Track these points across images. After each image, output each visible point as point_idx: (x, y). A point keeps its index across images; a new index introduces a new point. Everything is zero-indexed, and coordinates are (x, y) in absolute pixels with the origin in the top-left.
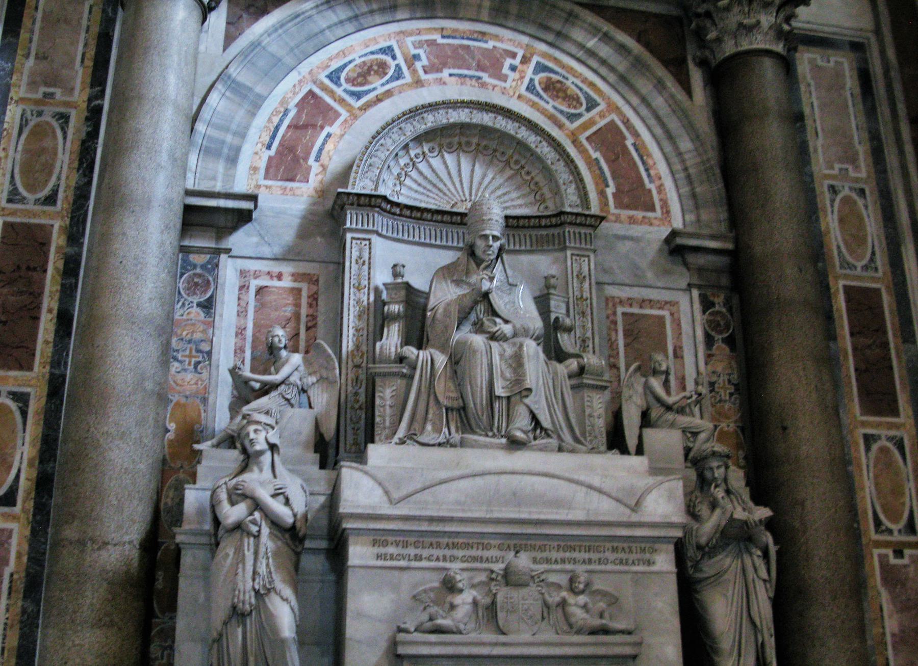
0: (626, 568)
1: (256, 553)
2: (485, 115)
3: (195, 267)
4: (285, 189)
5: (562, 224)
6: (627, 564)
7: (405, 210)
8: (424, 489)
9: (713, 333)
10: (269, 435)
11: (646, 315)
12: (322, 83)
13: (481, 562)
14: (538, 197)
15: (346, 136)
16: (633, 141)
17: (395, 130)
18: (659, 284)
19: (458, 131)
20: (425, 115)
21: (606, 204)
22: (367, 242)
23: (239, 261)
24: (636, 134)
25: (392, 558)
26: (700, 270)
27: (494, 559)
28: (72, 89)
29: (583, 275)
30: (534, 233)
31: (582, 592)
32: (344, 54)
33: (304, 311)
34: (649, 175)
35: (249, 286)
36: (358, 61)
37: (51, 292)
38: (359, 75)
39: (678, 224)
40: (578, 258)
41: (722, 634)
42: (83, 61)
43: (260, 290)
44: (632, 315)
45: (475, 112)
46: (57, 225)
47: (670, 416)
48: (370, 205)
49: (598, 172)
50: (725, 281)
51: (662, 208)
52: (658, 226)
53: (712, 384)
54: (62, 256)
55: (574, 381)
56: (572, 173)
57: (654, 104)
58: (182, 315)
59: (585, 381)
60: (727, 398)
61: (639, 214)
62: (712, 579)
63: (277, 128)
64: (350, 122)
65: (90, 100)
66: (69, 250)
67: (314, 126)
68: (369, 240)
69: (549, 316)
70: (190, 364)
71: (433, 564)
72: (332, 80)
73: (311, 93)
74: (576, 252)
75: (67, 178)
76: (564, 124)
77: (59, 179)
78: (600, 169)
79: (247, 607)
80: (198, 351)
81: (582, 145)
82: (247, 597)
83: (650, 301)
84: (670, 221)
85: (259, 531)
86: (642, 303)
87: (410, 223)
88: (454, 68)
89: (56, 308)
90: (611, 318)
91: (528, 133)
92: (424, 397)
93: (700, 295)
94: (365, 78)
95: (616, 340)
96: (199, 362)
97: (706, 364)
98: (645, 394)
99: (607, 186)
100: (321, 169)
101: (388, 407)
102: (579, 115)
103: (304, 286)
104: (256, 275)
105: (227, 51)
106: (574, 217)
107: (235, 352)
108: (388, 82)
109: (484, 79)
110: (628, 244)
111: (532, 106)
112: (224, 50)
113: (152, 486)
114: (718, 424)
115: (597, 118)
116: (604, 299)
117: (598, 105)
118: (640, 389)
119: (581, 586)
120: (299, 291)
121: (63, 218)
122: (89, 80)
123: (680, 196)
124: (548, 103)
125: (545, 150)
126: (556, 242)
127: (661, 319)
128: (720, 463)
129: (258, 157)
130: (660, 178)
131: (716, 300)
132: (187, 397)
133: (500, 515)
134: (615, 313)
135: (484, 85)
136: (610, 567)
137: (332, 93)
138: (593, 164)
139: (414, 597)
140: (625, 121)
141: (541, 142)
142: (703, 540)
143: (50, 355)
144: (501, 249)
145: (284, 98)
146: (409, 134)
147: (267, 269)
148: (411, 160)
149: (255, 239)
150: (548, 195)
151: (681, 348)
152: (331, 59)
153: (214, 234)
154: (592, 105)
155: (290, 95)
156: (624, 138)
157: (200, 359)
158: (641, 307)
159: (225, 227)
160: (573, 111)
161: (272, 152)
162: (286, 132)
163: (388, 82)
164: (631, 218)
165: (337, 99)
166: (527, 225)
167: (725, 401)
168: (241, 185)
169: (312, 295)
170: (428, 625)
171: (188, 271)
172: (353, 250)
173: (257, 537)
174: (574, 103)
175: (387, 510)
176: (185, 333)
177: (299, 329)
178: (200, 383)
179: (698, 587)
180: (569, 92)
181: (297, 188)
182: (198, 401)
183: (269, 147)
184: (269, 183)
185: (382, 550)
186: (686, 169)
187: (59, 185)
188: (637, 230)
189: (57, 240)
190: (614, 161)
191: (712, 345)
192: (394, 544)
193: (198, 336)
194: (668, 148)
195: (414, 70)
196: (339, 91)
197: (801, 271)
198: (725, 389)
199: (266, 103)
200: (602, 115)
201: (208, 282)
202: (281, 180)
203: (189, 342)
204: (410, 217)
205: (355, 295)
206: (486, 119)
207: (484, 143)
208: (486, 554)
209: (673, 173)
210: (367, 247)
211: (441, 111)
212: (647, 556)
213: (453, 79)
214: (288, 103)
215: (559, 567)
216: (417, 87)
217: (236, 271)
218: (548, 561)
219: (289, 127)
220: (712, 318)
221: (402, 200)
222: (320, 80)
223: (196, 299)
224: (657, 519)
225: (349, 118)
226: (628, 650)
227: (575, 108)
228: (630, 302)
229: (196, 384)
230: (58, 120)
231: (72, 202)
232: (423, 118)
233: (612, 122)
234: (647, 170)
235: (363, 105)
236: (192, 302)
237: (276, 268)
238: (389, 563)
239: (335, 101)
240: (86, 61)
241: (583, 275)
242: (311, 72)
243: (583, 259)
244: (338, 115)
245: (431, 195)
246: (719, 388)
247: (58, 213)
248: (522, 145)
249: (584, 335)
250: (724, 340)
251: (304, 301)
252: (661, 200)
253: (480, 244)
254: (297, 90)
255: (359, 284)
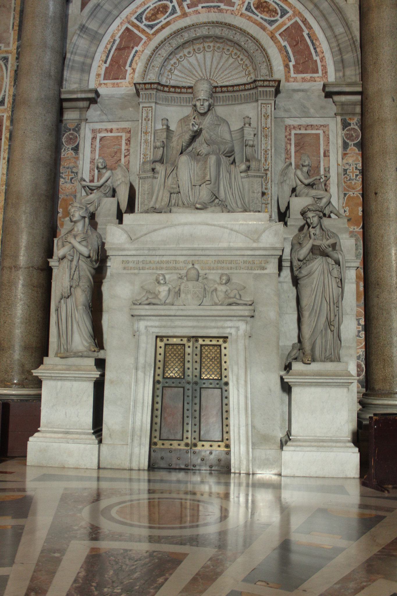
0: (250, 271)
1: (71, 269)
2: (216, 29)
3: (70, 130)
4: (114, 84)
5: (256, 87)
6: (251, 269)
7: (171, 89)
8: (146, 234)
9: (348, 141)
10: (80, 213)
11: (308, 134)
12: (133, 22)
13: (175, 270)
14: (247, 73)
15: (145, 51)
16: (308, 32)
17: (166, 45)
18: (318, 116)
19: (202, 40)
20: (183, 34)
21: (289, 72)
22: (151, 109)
23: (91, 124)
24: (310, 28)
25: (131, 269)
26: (343, 104)
27: (182, 268)
28: (9, 43)
29: (267, 114)
30: (242, 93)
31: (226, 283)
32: (144, 4)
33: (124, 147)
34: (316, 52)
35: (96, 138)
36: (152, 7)
37: (4, 149)
38: (153, 15)
39: (331, 78)
40: (265, 105)
41: (306, 306)
42: (13, 28)
43: (101, 139)
44: (301, 134)
45: (211, 28)
46: (5, 115)
47: (306, 190)
48: (151, 89)
49: (285, 53)
50: (358, 109)
51: (322, 70)
52: (320, 81)
53: (345, 170)
54: (8, 131)
55: (243, 175)
56: (264, 56)
57: (321, 8)
58: (64, 155)
59: (249, 174)
60: (354, 177)
61: (308, 76)
62: (306, 277)
63: (110, 51)
64: (147, 43)
65: (18, 48)
66: (11, 127)
67: (128, 47)
68: (151, 107)
69: (243, 139)
70: (68, 179)
71: (151, 271)
72: (138, 20)
73: (127, 29)
74: (264, 102)
75: (9, 90)
76: (267, 27)
77: (5, 92)
78: (287, 52)
79: (66, 295)
80: (72, 172)
81: (277, 39)
82: (66, 290)
83: (312, 125)
84: (327, 78)
85: (73, 259)
86: (307, 127)
87: (175, 95)
88: (204, 3)
89: (7, 157)
90: (288, 137)
91: (240, 36)
92: (162, 187)
93: (342, 120)
94: (156, 16)
95: (290, 149)
96: (73, 178)
97: (343, 159)
98: (295, 179)
99: (290, 61)
100: (132, 71)
101: (146, 194)
102: (276, 21)
103: (124, 136)
104: (100, 131)
105: (82, 12)
106: (262, 82)
107: (90, 171)
108: (168, 17)
109: (221, 7)
110: (301, 94)
111: (248, 19)
112: (81, 11)
113: (44, 240)
114: (347, 192)
115: (287, 21)
116: (284, 127)
117: (288, 12)
118: (292, 176)
119: (224, 282)
120: (121, 137)
121: (8, 111)
122: (16, 37)
123: (334, 62)
124: (258, 16)
125: (251, 46)
126: (254, 97)
127: (318, 135)
128: (314, 215)
129: (100, 68)
130: (323, 53)
131: (352, 122)
132: (67, 196)
133: (183, 246)
134: (290, 134)
135: (221, 11)
136: (241, 271)
137: (137, 27)
138: (282, 49)
139: (142, 287)
140: (304, 20)
141: (247, 40)
142: (301, 258)
143: (5, 180)
144: (210, 106)
145: (113, 33)
146: (174, 46)
147: (105, 128)
148: (178, 60)
149: (99, 113)
150: (252, 71)
151: (328, 151)
152: (137, 8)
153: (79, 112)
154: (284, 13)
155: (116, 31)
156: (302, 31)
157: (73, 176)
158: (306, 130)
159: (84, 108)
160: (273, 19)
161: (107, 65)
162: (114, 53)
163: (168, 17)
164: (303, 78)
165: (141, 31)
166: (238, 89)
167: (353, 180)
168: (92, 85)
169: (127, 139)
170: (147, 302)
171: (67, 132)
172: (143, 114)
173: (71, 261)
174: (274, 14)
175: (127, 246)
176: (66, 164)
177: (121, 157)
178: (73, 188)
179: (299, 282)
180: (270, 8)
181: (121, 83)
182: (72, 197)
183: (105, 62)
184: (106, 82)
185: (127, 265)
186: (339, 45)
187: (5, 95)
188: (306, 86)
189: (6, 123)
190: (295, 46)
191: (347, 148)
192: (132, 262)
193: (72, 165)
194: (329, 33)
195: (182, 7)
196: (142, 26)
197: (394, 100)
198: (353, 172)
199: (104, 38)
200: (289, 19)
201: (77, 137)
202: (112, 79)
203: (68, 168)
204: (175, 92)
205: (144, 136)
206: (217, 31)
207: (218, 45)
208: (178, 265)
209: (331, 49)
210: (151, 111)
211: (192, 30)
212: (263, 265)
213: (204, 9)
214: (115, 36)
215: (214, 272)
216: (184, 18)
217: (90, 130)
218: (209, 269)
219: (116, 50)
220: (348, 132)
221: (173, 83)
222: (132, 21)
223: (70, 147)
224: (268, 246)
225: (147, 41)
226: (247, 313)
227: (274, 16)
228: (300, 127)
229: (71, 189)
230: (3, 61)
231: (11, 103)
232: (182, 36)
233: (296, 22)
234: (315, 49)
235: (154, 32)
236: (69, 148)
237: (109, 126)
238: (129, 272)
239: (140, 32)
240: (15, 27)
241: (267, 114)
242: (126, 18)
243: (268, 105)
244: (141, 39)
245: (188, 78)
246: (349, 172)
247: (6, 109)
248: (237, 44)
249: (266, 148)
250: (354, 145)
251: (124, 142)
252: (322, 66)
253: (198, 104)
254: (120, 28)
255: (146, 132)
